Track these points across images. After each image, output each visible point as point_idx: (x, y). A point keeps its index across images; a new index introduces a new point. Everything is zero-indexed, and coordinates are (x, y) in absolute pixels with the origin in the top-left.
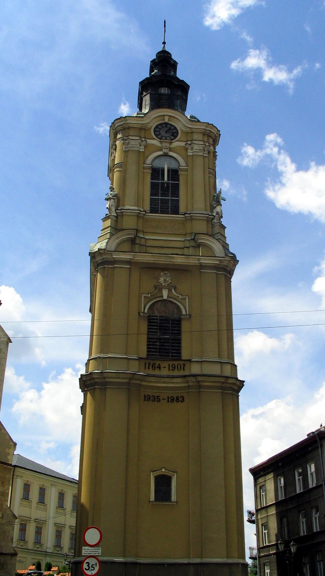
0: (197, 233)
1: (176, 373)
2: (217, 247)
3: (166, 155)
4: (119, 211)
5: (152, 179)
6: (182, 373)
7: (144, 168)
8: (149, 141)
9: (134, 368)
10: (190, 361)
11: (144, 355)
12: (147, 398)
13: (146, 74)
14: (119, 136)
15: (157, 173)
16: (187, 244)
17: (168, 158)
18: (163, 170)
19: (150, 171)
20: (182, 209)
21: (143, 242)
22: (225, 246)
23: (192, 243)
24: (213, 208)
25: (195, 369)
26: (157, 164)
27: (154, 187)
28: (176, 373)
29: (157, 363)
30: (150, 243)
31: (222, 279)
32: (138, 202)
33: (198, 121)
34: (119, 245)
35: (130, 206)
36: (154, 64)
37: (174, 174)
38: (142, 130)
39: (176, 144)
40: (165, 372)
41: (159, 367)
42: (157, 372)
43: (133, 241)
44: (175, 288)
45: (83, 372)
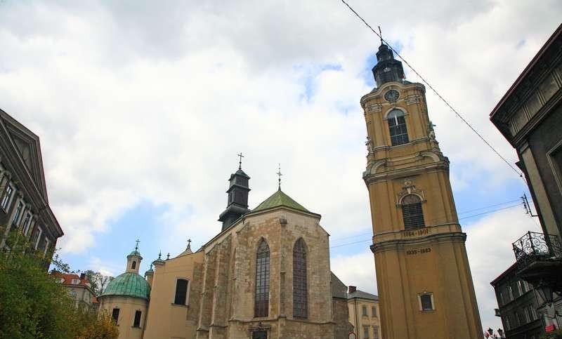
0: (423, 151)
1: (423, 235)
2: (436, 159)
3: (394, 109)
5: (389, 126)
6: (427, 235)
9: (399, 237)
10: (430, 227)
11: (403, 229)
12: (409, 253)
13: (375, 63)
14: (366, 105)
15: (391, 121)
16: (417, 159)
17: (396, 111)
18: (395, 119)
19: (387, 121)
20: (410, 139)
21: (391, 164)
22: (440, 155)
23: (420, 158)
24: (428, 133)
25: (434, 232)
26: (391, 117)
27: (391, 130)
28: (423, 235)
29: (412, 232)
30: (396, 164)
31: (441, 174)
32: (384, 140)
33: (410, 83)
34: (377, 169)
35: (379, 145)
36: (378, 55)
37: (401, 119)
38: (378, 98)
39: (399, 101)
40: (417, 236)
41: (413, 234)
42: (412, 237)
43: (385, 165)
44: (414, 186)
45: (372, 244)
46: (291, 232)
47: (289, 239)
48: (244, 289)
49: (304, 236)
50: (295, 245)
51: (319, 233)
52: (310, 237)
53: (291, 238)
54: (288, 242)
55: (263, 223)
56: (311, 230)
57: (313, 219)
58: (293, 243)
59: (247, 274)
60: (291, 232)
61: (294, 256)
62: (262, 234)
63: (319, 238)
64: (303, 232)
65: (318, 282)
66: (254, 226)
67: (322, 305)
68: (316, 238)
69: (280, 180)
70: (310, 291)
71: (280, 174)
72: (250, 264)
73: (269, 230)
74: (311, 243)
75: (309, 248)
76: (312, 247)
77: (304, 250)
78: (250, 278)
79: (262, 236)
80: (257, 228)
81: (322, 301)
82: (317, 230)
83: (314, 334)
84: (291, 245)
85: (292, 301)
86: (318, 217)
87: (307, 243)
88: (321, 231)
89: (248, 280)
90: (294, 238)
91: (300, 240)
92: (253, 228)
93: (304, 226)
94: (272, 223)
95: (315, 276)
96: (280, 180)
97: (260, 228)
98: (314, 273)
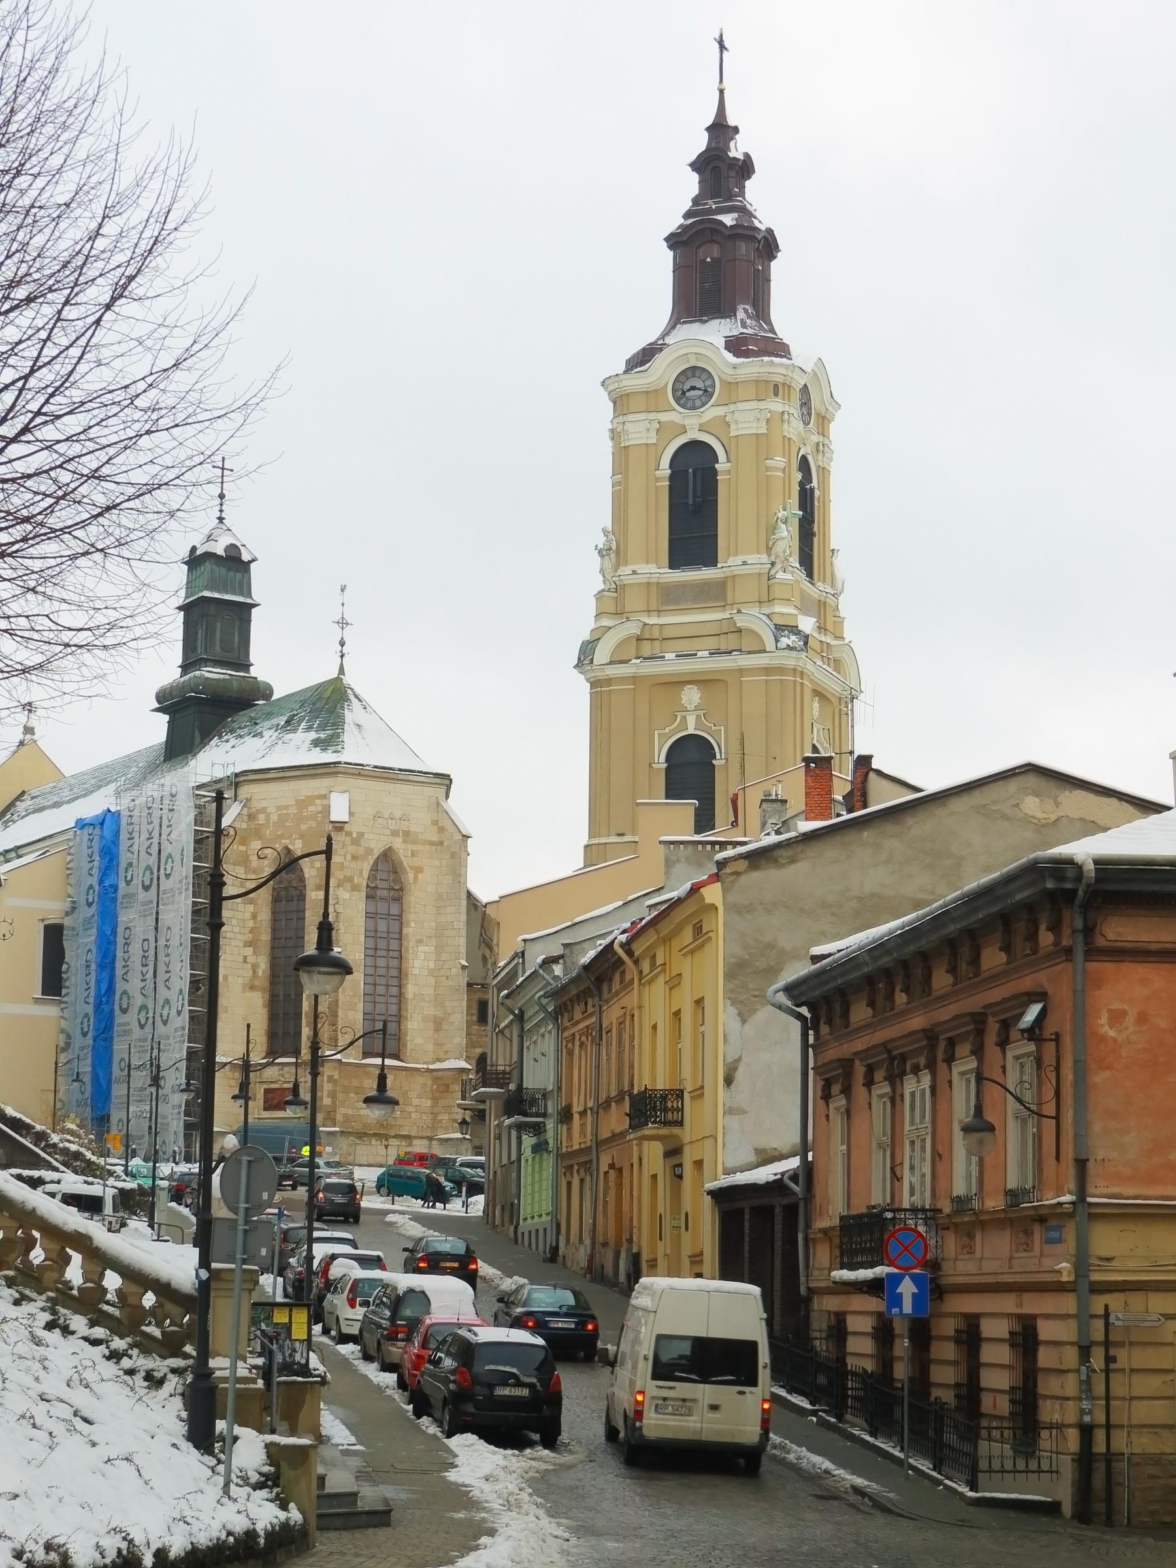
4: (617, 579)
7: (657, 480)
8: (665, 417)
46: (361, 835)
47: (354, 858)
48: (240, 981)
49: (398, 844)
50: (374, 869)
51: (441, 830)
52: (414, 843)
53: (361, 851)
54: (353, 865)
55: (287, 807)
56: (421, 823)
57: (430, 791)
58: (366, 866)
59: (248, 944)
60: (361, 835)
61: (369, 897)
62: (282, 837)
63: (441, 843)
64: (394, 833)
65: (432, 965)
66: (263, 810)
67: (438, 1024)
68: (431, 843)
69: (342, 644)
70: (410, 990)
71: (343, 623)
72: (254, 916)
73: (303, 827)
74: (416, 862)
75: (411, 875)
76: (419, 870)
77: (398, 881)
78: (255, 952)
79: (285, 842)
80: (274, 818)
81: (439, 1014)
82: (435, 823)
83: (410, 1094)
84: (361, 872)
85: (360, 1016)
86: (444, 780)
87: (406, 862)
88: (447, 824)
89: (251, 959)
90: (369, 851)
91: (387, 856)
92: (261, 818)
93: (398, 814)
94: (311, 808)
95: (426, 949)
96: (342, 644)
97: (282, 819)
98: (420, 942)
